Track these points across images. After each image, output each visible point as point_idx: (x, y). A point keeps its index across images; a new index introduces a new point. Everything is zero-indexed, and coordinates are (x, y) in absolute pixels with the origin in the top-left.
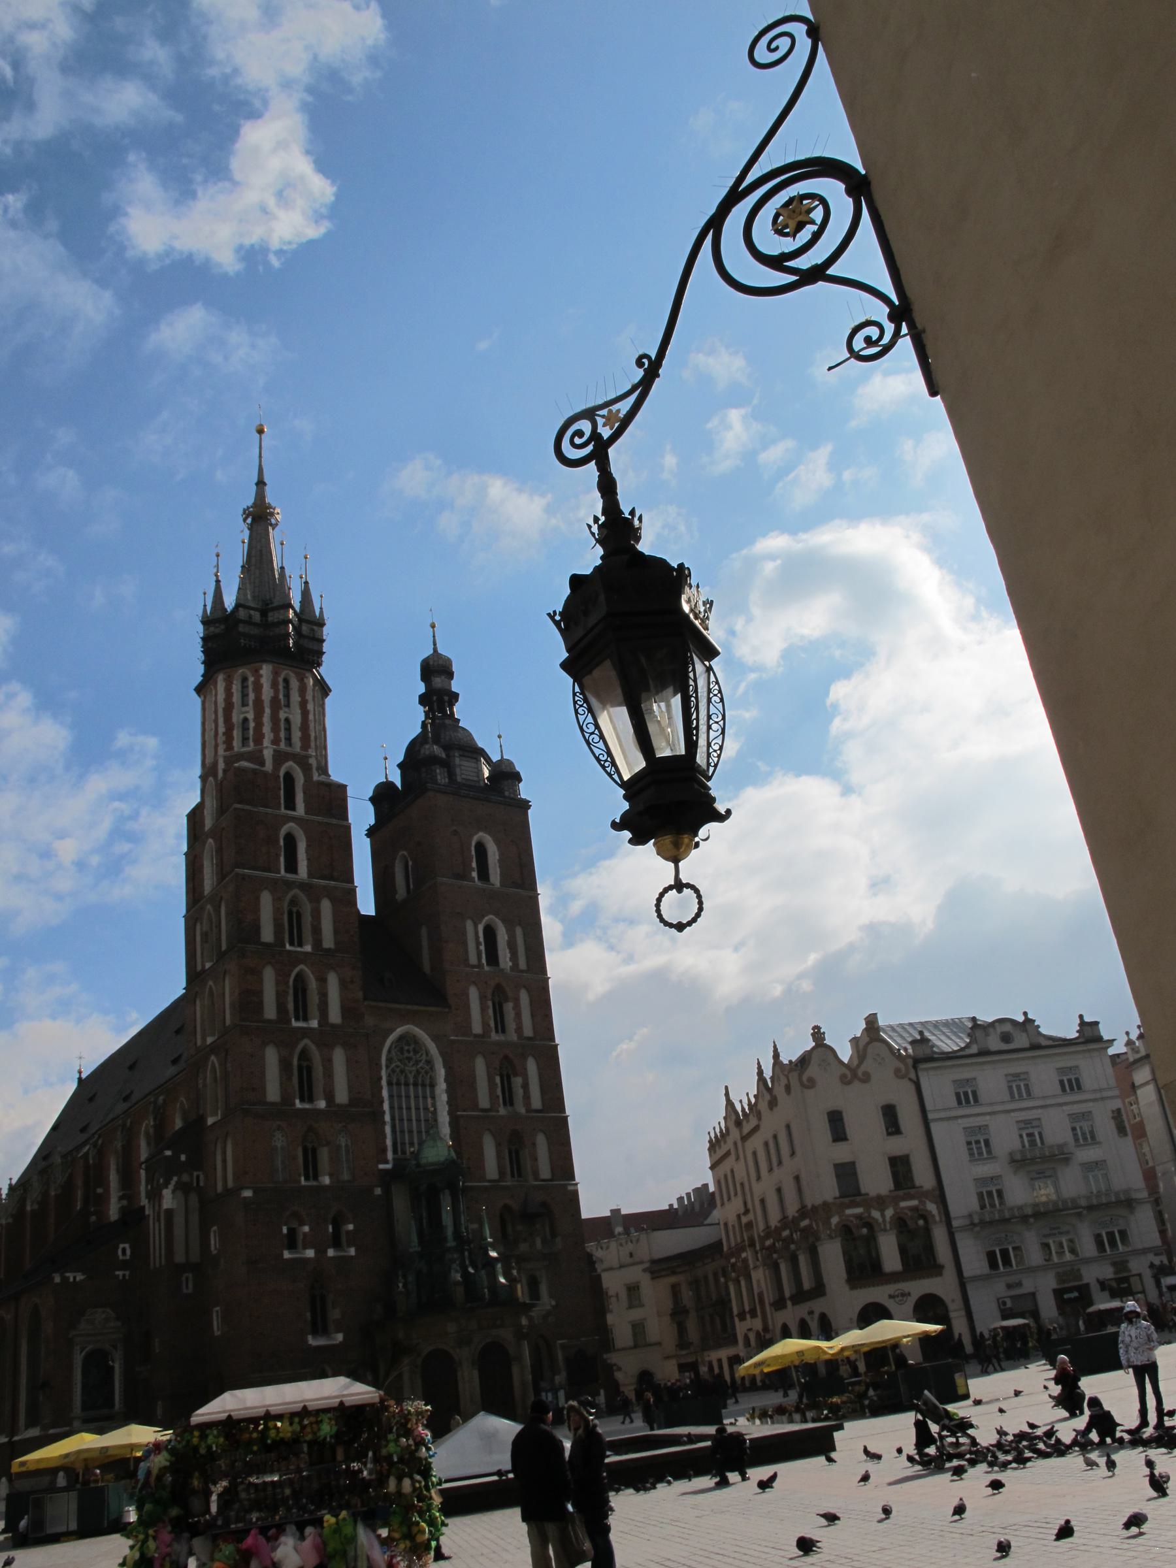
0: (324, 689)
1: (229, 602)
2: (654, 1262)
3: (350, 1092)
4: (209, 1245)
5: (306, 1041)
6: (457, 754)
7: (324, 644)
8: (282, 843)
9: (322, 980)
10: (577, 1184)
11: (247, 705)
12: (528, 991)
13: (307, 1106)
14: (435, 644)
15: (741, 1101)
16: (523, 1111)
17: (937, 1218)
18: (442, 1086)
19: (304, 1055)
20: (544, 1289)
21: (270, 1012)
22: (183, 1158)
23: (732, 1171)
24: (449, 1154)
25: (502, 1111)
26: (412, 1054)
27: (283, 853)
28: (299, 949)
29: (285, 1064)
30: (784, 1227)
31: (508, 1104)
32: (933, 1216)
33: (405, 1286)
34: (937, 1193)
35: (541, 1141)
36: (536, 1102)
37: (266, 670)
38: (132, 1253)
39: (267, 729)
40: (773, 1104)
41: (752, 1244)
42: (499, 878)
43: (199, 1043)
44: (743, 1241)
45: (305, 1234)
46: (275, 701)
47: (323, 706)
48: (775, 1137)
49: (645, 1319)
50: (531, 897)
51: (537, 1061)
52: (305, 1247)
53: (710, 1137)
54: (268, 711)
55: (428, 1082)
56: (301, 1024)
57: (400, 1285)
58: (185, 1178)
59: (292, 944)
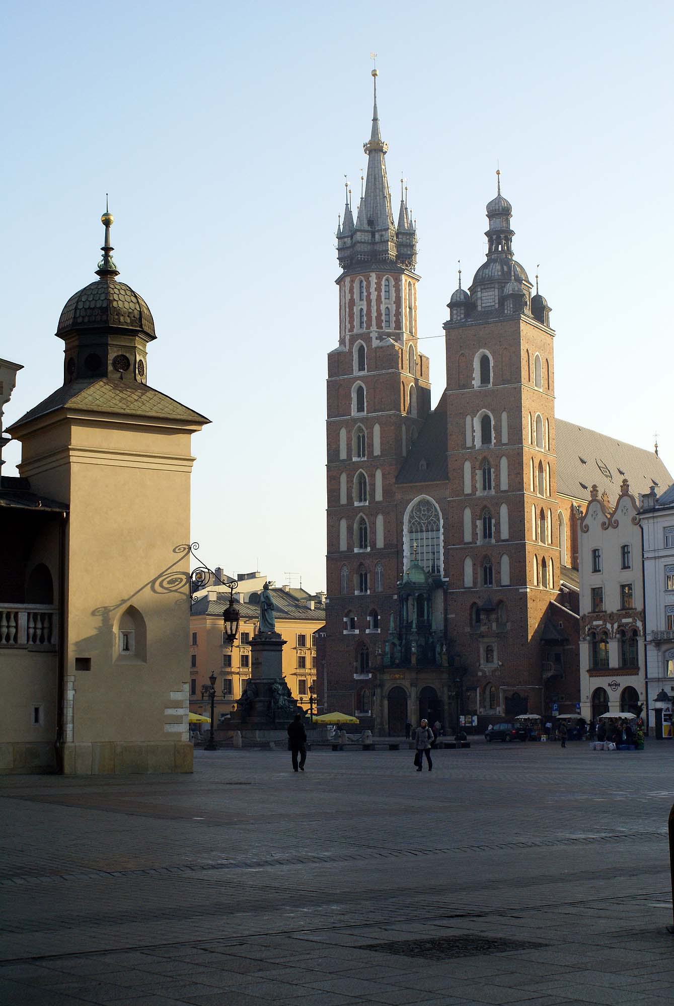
5: (361, 513)
6: (479, 290)
9: (373, 476)
12: (506, 457)
13: (361, 551)
16: (493, 541)
17: (642, 634)
19: (362, 521)
20: (495, 654)
21: (344, 500)
26: (426, 513)
32: (640, 631)
34: (642, 614)
36: (505, 534)
54: (347, 310)
56: (362, 504)
59: (359, 456)
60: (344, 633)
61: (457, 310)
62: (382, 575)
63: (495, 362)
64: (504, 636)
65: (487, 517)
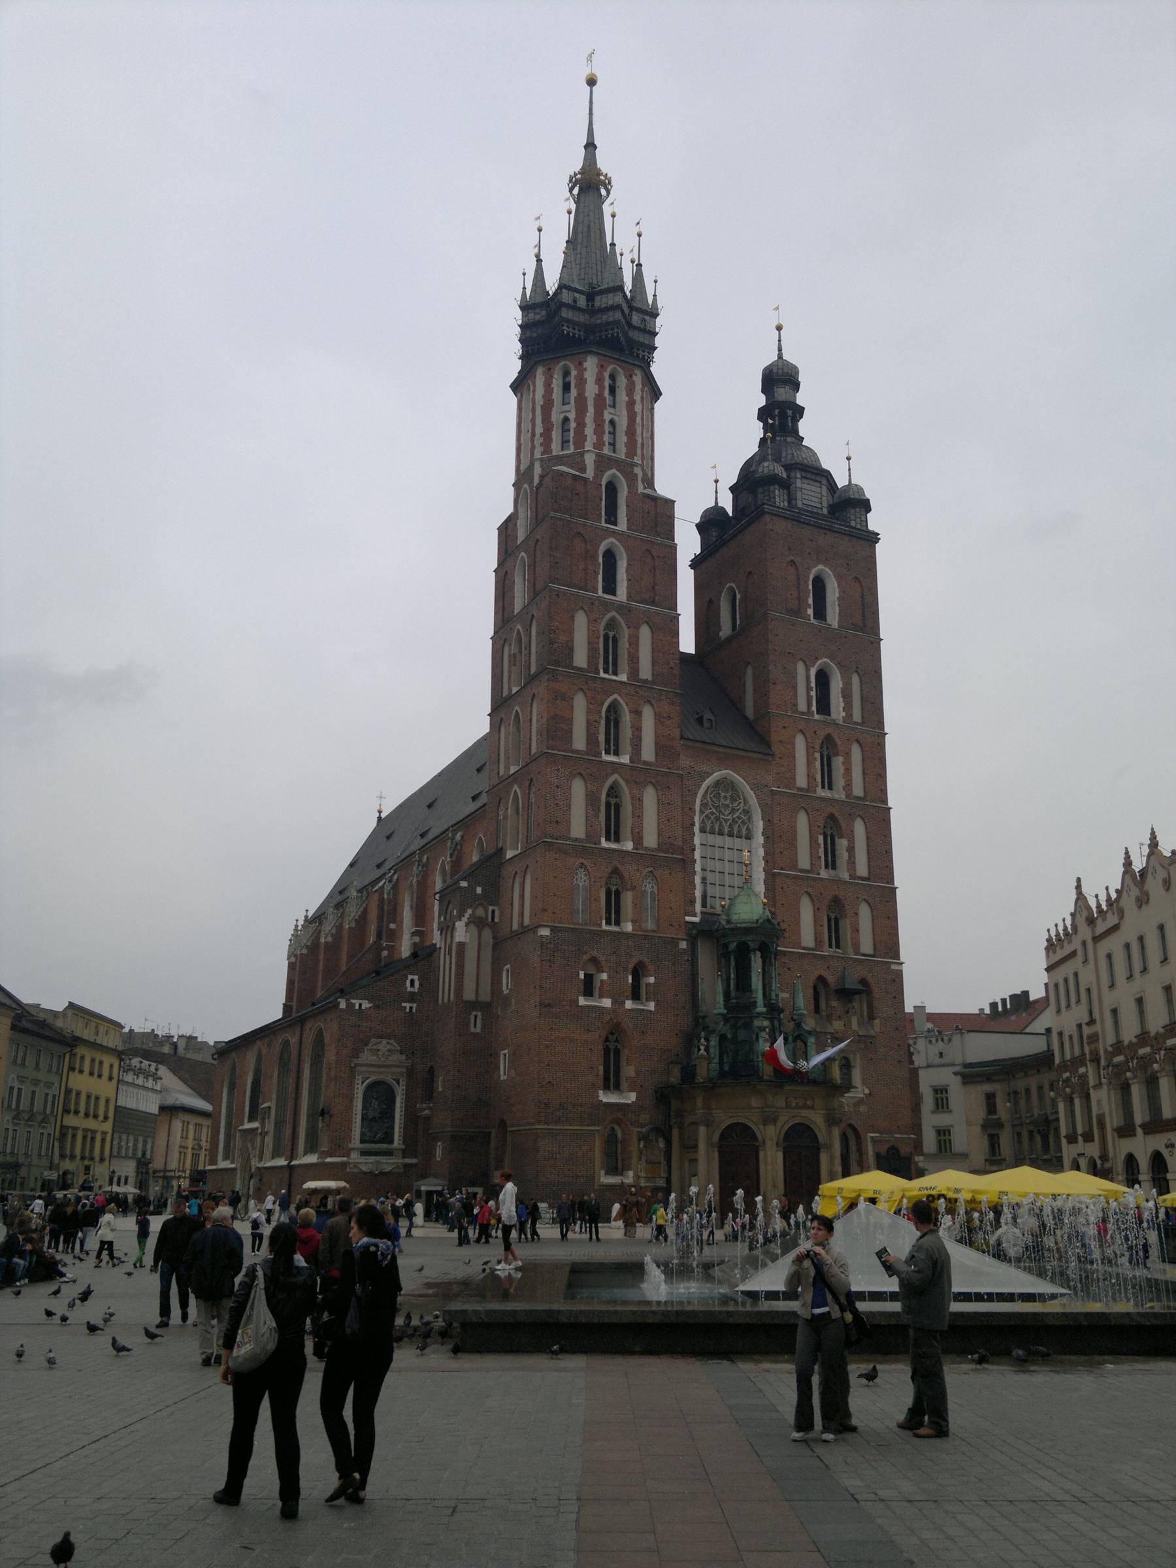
0: (656, 394)
1: (552, 283)
2: (966, 1065)
3: (659, 835)
4: (501, 983)
5: (616, 775)
7: (656, 338)
8: (601, 560)
9: (637, 713)
10: (902, 963)
11: (569, 403)
12: (860, 745)
13: (613, 846)
14: (780, 350)
15: (1097, 896)
16: (846, 876)
18: (759, 839)
19: (614, 791)
20: (857, 1077)
21: (579, 742)
22: (479, 890)
23: (1076, 975)
24: (764, 913)
25: (824, 874)
26: (728, 802)
27: (601, 571)
28: (614, 677)
29: (592, 800)
30: (1144, 1045)
31: (830, 868)
33: (707, 1050)
35: (864, 911)
37: (591, 364)
38: (421, 985)
39: (589, 430)
40: (1142, 901)
41: (1096, 1060)
42: (837, 619)
43: (502, 773)
44: (1084, 1054)
45: (602, 981)
46: (599, 398)
47: (653, 408)
48: (1141, 939)
49: (952, 1126)
50: (872, 643)
51: (865, 823)
52: (601, 996)
53: (1050, 935)
54: (591, 410)
55: (744, 832)
56: (611, 758)
57: (702, 1048)
58: (480, 912)
59: (606, 671)
60: (580, 1004)
61: (779, 490)
62: (653, 899)
63: (842, 591)
64: (871, 1043)
65: (829, 833)
